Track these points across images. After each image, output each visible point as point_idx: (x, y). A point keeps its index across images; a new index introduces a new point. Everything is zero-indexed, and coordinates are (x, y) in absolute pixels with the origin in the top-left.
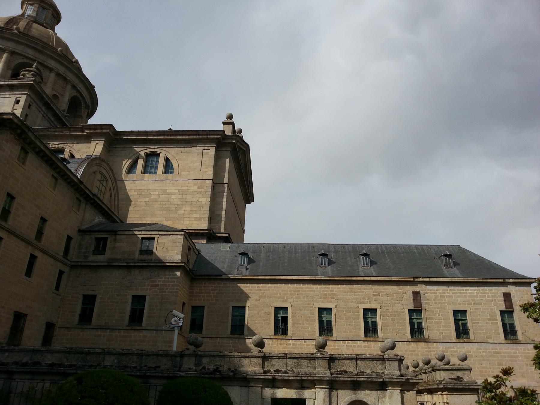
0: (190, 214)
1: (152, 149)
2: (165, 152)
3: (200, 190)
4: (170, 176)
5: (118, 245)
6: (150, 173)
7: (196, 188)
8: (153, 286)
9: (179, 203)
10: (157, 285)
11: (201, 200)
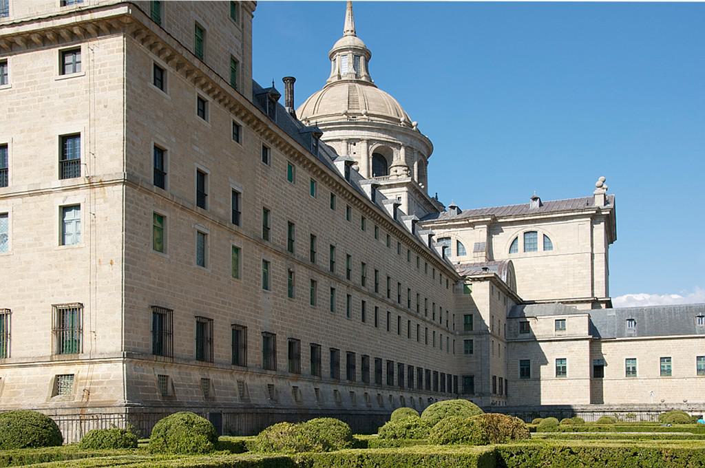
0: (573, 284)
1: (530, 227)
2: (542, 229)
3: (580, 263)
4: (550, 252)
5: (538, 326)
6: (530, 250)
7: (576, 261)
8: (569, 352)
9: (563, 275)
10: (573, 351)
11: (581, 271)
